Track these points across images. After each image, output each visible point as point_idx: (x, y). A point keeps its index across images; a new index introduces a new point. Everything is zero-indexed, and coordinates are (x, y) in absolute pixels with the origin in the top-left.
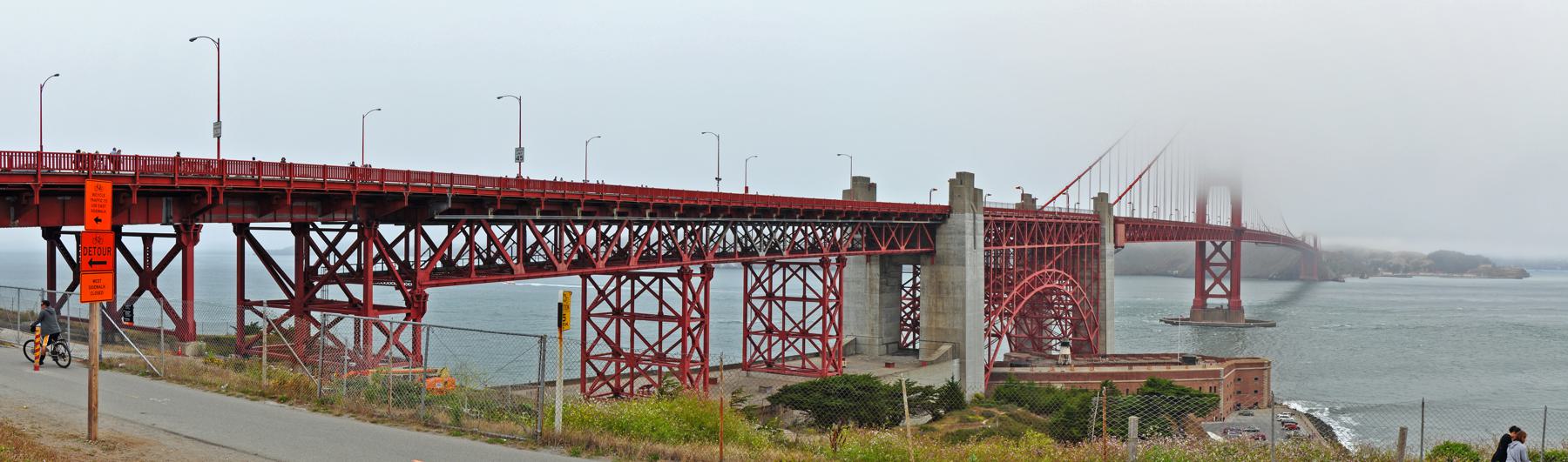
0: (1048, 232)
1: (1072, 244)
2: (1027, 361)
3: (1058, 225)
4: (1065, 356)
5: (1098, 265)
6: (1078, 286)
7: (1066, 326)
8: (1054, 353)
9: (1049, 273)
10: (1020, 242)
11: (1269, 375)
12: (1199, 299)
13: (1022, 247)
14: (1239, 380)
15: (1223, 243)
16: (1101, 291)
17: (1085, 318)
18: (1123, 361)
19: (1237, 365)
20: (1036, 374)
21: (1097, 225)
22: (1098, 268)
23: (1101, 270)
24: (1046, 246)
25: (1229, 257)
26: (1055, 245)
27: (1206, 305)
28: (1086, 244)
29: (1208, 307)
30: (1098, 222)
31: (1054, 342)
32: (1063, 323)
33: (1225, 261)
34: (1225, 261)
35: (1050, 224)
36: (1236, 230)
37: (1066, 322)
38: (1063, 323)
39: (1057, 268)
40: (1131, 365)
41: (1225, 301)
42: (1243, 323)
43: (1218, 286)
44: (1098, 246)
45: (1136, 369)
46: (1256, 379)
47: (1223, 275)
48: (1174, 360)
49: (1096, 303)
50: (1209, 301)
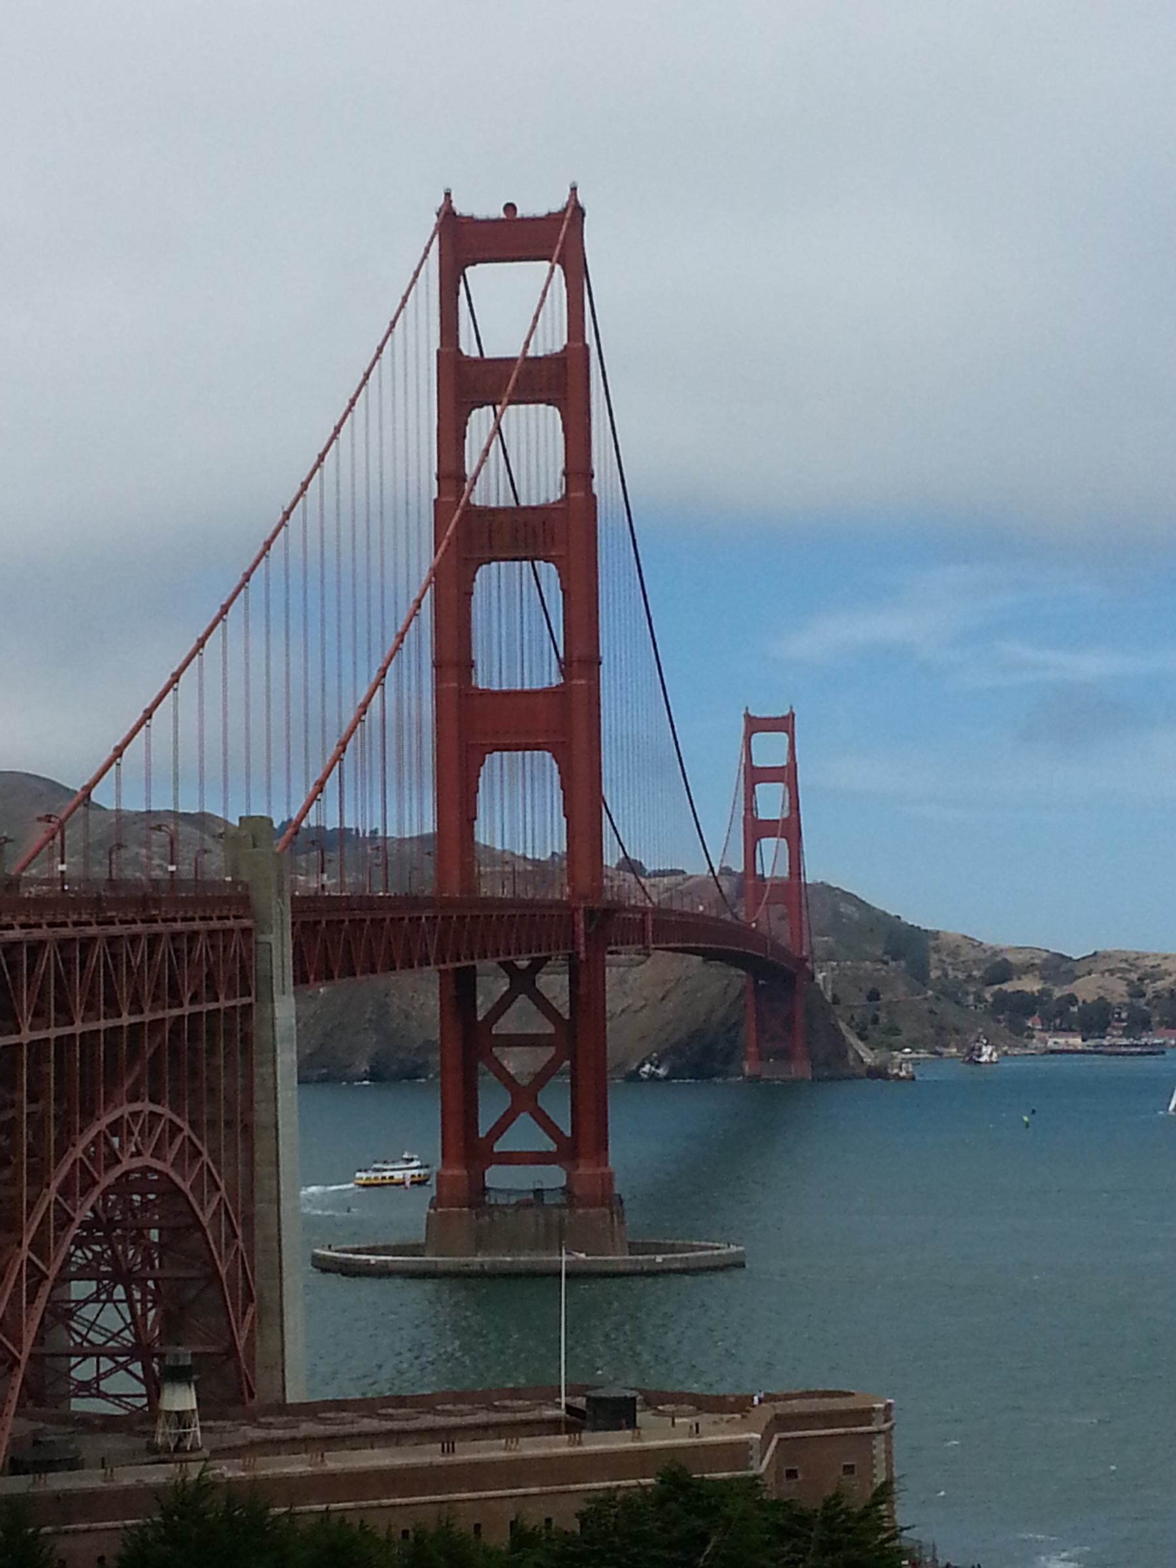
0: (129, 967)
1: (187, 1009)
2: (36, 1443)
3: (154, 939)
4: (181, 1418)
5: (249, 1077)
6: (206, 1157)
7: (143, 1301)
8: (79, 1405)
9: (135, 1115)
10: (65, 1015)
11: (889, 1452)
12: (458, 1171)
13: (68, 1030)
14: (792, 1474)
15: (537, 966)
16: (261, 1170)
17: (223, 1271)
18: (369, 1424)
19: (781, 1422)
20: (127, 1492)
21: (247, 932)
22: (249, 1090)
23: (258, 1095)
24: (126, 1020)
26: (147, 1017)
27: (485, 1190)
28: (223, 1003)
29: (490, 1199)
30: (247, 923)
31: (84, 1371)
32: (137, 1295)
33: (550, 1029)
34: (550, 1029)
35: (135, 939)
36: (590, 914)
37: (145, 1291)
38: (137, 1295)
39: (151, 1100)
40: (446, 1436)
41: (554, 1176)
42: (620, 1259)
43: (524, 1118)
44: (250, 1005)
45: (469, 1452)
46: (849, 1469)
47: (542, 1078)
48: (550, 1413)
49: (248, 1221)
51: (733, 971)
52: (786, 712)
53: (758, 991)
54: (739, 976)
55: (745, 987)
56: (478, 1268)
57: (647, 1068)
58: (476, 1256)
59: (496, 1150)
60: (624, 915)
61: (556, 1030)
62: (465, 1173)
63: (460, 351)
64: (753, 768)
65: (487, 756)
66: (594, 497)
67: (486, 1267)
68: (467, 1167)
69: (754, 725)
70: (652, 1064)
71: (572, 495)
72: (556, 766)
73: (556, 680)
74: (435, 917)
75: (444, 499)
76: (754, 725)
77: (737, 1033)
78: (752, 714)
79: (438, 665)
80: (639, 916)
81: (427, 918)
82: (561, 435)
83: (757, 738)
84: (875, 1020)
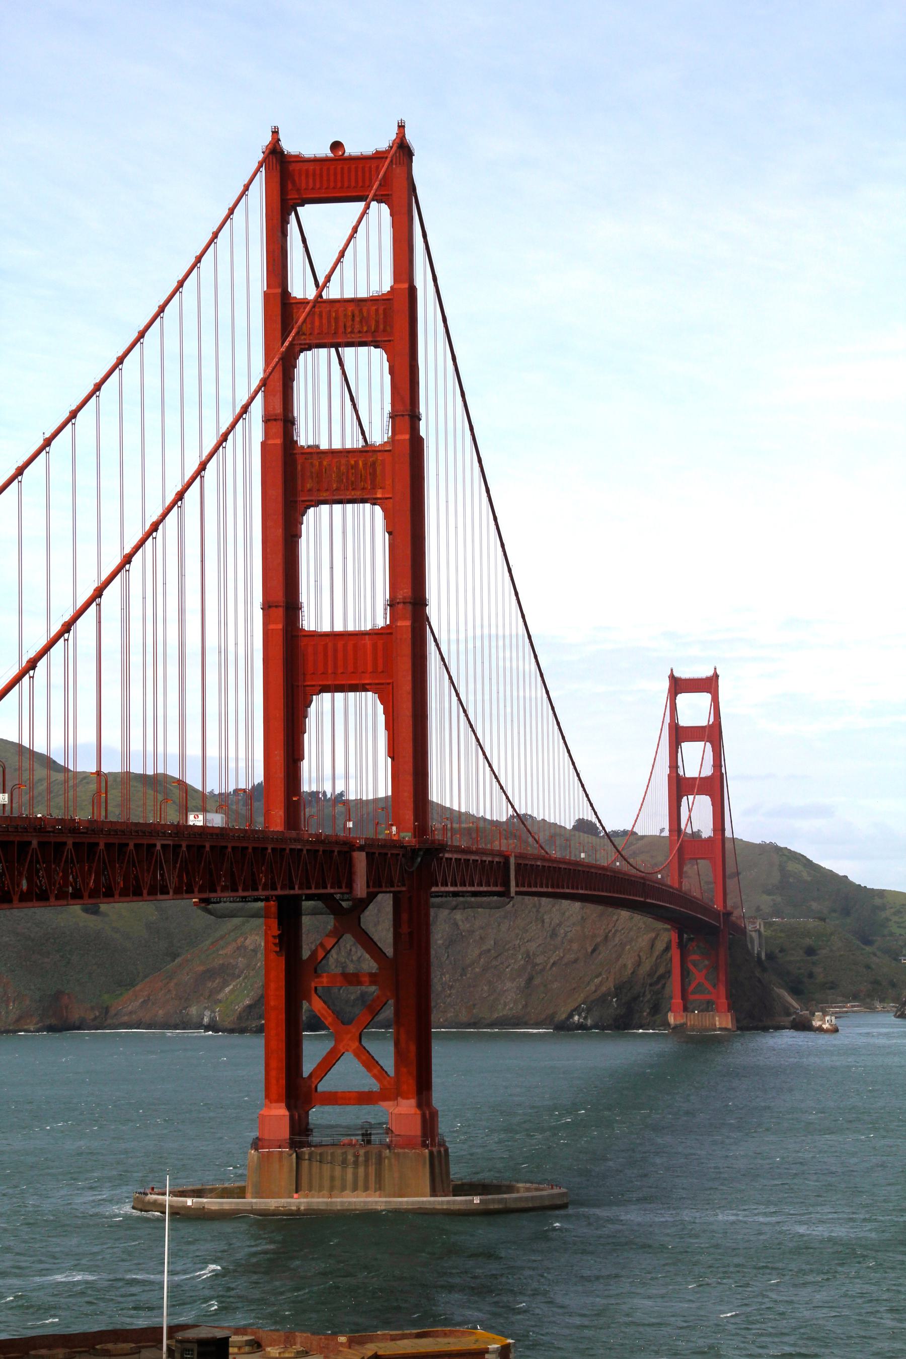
12: (281, 1111)
25: (389, 951)
50: (318, 1115)
51: (660, 925)
52: (709, 673)
53: (682, 946)
54: (666, 930)
55: (670, 941)
56: (294, 1208)
57: (576, 1018)
58: (292, 1197)
59: (321, 1088)
60: (447, 855)
61: (380, 968)
62: (287, 1113)
63: (285, 294)
64: (677, 725)
65: (314, 697)
66: (421, 439)
67: (302, 1208)
68: (288, 1107)
69: (678, 686)
70: (579, 1015)
71: (398, 437)
72: (380, 708)
73: (381, 620)
74: (177, 847)
75: (270, 442)
76: (678, 686)
77: (665, 984)
78: (677, 674)
79: (267, 607)
80: (502, 860)
81: (163, 846)
82: (388, 378)
83: (683, 699)
84: (811, 975)
